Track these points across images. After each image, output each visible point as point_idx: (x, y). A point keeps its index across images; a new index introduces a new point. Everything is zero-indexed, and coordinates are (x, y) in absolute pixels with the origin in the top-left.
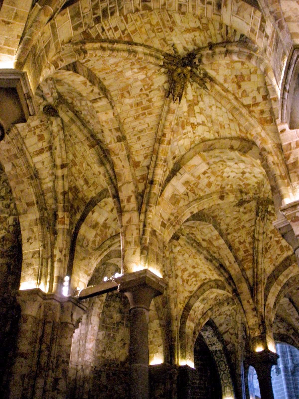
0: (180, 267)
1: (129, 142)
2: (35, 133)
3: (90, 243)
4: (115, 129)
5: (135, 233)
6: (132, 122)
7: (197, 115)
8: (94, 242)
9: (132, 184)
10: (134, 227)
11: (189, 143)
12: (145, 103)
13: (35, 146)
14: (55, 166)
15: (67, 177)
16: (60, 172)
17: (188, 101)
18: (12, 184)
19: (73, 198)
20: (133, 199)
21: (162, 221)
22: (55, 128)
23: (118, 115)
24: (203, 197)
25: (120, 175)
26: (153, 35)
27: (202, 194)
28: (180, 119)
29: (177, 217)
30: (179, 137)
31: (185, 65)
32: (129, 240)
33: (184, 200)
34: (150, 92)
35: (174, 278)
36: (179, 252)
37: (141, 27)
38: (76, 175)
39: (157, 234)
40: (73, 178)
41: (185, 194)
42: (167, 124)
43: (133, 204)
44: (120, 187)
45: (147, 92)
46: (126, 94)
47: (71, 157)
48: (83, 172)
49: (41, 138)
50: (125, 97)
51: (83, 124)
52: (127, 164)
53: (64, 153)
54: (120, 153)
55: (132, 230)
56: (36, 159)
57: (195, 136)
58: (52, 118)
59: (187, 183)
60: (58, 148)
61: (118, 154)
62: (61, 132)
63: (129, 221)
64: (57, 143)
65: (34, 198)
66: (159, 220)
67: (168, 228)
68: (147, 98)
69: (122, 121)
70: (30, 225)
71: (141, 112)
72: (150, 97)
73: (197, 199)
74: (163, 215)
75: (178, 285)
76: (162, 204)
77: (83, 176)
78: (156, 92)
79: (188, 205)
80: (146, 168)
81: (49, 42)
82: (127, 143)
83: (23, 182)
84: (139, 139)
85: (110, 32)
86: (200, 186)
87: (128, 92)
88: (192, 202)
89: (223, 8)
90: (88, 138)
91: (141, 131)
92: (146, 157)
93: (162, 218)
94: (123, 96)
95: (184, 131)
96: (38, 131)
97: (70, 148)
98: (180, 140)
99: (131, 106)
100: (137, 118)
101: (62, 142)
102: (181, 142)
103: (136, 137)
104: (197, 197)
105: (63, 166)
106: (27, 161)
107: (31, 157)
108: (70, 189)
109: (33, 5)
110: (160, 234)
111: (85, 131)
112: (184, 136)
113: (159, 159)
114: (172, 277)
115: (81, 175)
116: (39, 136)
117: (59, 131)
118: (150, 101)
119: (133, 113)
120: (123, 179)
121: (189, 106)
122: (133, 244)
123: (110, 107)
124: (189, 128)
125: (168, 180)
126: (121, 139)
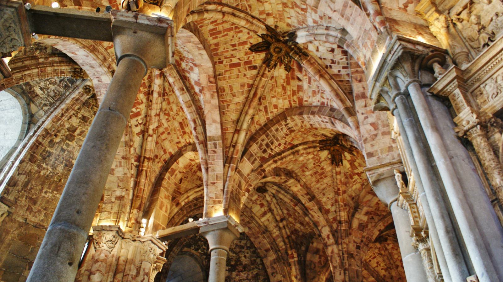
0: (397, 258)
1: (318, 198)
2: (257, 204)
3: (317, 265)
4: (305, 194)
5: (338, 259)
6: (315, 185)
7: (358, 167)
8: (320, 262)
9: (327, 226)
10: (336, 256)
11: (360, 186)
12: (320, 171)
13: (260, 211)
14: (276, 221)
15: (287, 226)
16: (281, 225)
17: (349, 161)
18: (252, 239)
19: (296, 238)
20: (331, 236)
21: (357, 245)
22: (269, 199)
23: (305, 183)
24: (386, 215)
25: (318, 222)
26: (306, 135)
27: (384, 214)
28: (348, 174)
29: (368, 237)
30: (351, 185)
31: (335, 145)
32: (335, 265)
33: (371, 222)
34: (320, 163)
35: (395, 268)
36: (392, 248)
37: (296, 135)
38: (293, 222)
39: (354, 256)
40: (291, 225)
41: (371, 219)
42: (338, 182)
43: (332, 240)
44: (321, 230)
45: (319, 164)
46: (305, 169)
47: (285, 212)
48: (298, 218)
49: (262, 205)
50: (305, 171)
51: (286, 192)
52: (320, 214)
53: (280, 212)
54: (314, 208)
55: (335, 258)
56: (263, 219)
57: (363, 180)
58: (265, 194)
59: (367, 213)
60: (275, 210)
61: (312, 209)
62: (274, 199)
63: (332, 252)
64: (273, 206)
65: (269, 246)
66: (354, 246)
67: (363, 248)
68: (320, 168)
69: (309, 186)
70: (271, 264)
71: (319, 177)
72: (321, 166)
73: (381, 219)
74: (356, 240)
75: (400, 273)
76: (353, 233)
77: (299, 221)
78: (325, 162)
79: (375, 226)
80: (334, 213)
81: (240, 182)
82: (317, 199)
83: (259, 237)
84: (324, 194)
85: (277, 148)
86: (381, 209)
87: (306, 168)
88: (377, 222)
89: (335, 125)
90: (291, 200)
91: (323, 189)
92: (332, 205)
93: (356, 243)
94: (304, 171)
95: (353, 180)
96: (258, 202)
97: (283, 207)
98: (352, 186)
99: (311, 175)
100: (318, 182)
101: (276, 205)
102: (354, 187)
103: (322, 194)
104: (381, 217)
105: (282, 220)
106: (257, 222)
107: (260, 219)
108: (292, 233)
109: (224, 166)
110: (357, 255)
111: (288, 196)
112: (354, 183)
113: (340, 205)
114: (393, 268)
115: (297, 221)
116: (260, 204)
117: (272, 199)
118: (322, 169)
119: (314, 179)
120: (321, 224)
121: (350, 164)
122: (338, 268)
123: (296, 182)
124: (356, 177)
125: (353, 215)
126: (312, 198)
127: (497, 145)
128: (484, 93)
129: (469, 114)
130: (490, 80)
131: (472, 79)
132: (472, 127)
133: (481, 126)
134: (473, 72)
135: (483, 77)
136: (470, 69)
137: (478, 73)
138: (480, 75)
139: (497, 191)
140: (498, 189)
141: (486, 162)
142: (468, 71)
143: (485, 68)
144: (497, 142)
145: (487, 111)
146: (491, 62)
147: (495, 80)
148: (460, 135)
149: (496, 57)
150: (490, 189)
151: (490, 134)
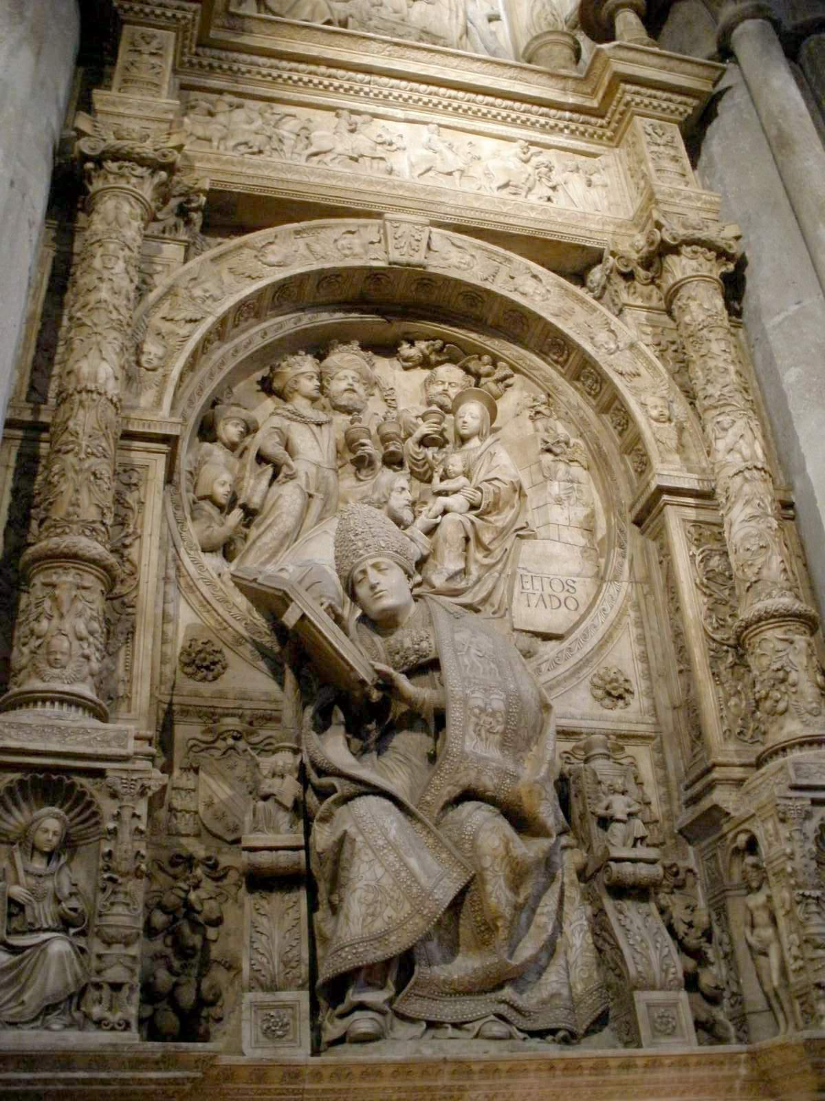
127: (151, 275)
128: (221, 118)
129: (160, 121)
130: (261, 104)
131: (223, 54)
132: (141, 161)
133: (163, 184)
134: (246, 40)
135: (252, 82)
136: (248, 24)
137: (255, 58)
138: (255, 69)
139: (77, 397)
140: (84, 395)
141: (104, 286)
142: (238, 23)
143: (284, 64)
144: (159, 268)
145: (198, 164)
146: (313, 68)
147: (278, 117)
148: (84, 146)
149: (333, 71)
150: (26, 381)
151: (155, 228)
